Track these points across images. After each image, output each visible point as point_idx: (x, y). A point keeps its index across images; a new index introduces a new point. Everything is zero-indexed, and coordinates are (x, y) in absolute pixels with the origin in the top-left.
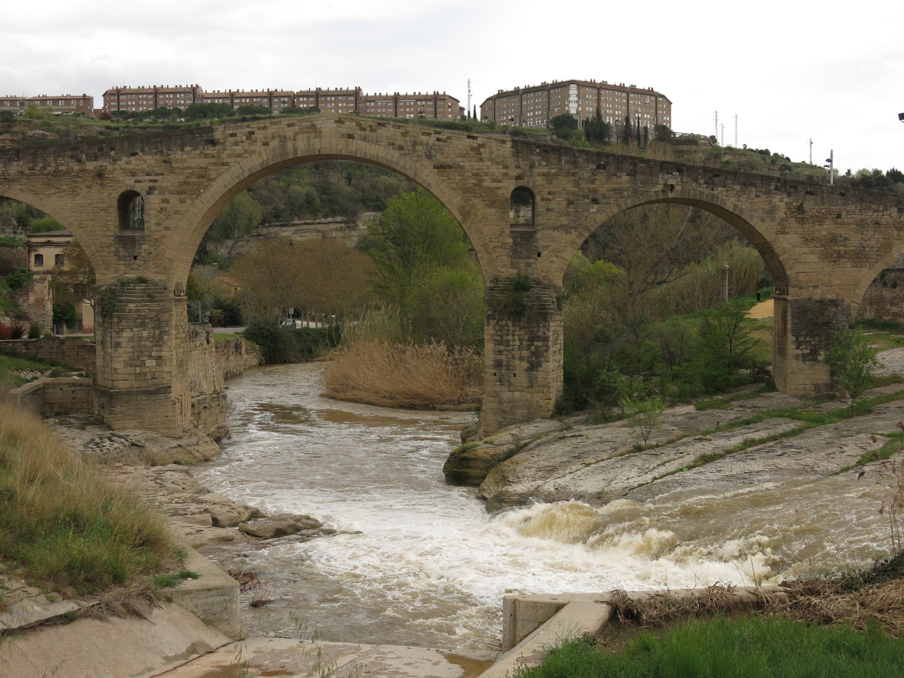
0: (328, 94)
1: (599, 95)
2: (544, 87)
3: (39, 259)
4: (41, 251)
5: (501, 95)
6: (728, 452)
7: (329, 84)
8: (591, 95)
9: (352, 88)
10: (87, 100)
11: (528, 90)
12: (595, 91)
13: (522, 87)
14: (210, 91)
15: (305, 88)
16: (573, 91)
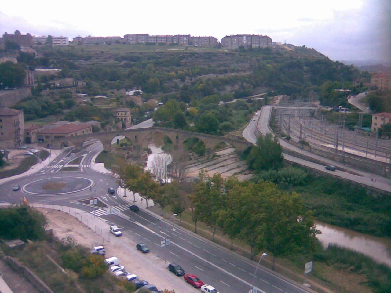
0: (182, 36)
1: (251, 39)
2: (238, 36)
3: (118, 114)
4: (119, 113)
5: (227, 37)
6: (192, 167)
7: (182, 34)
8: (249, 39)
9: (188, 35)
10: (119, 38)
11: (234, 36)
12: (250, 37)
13: (232, 35)
14: (151, 35)
15: (176, 35)
16: (245, 37)
